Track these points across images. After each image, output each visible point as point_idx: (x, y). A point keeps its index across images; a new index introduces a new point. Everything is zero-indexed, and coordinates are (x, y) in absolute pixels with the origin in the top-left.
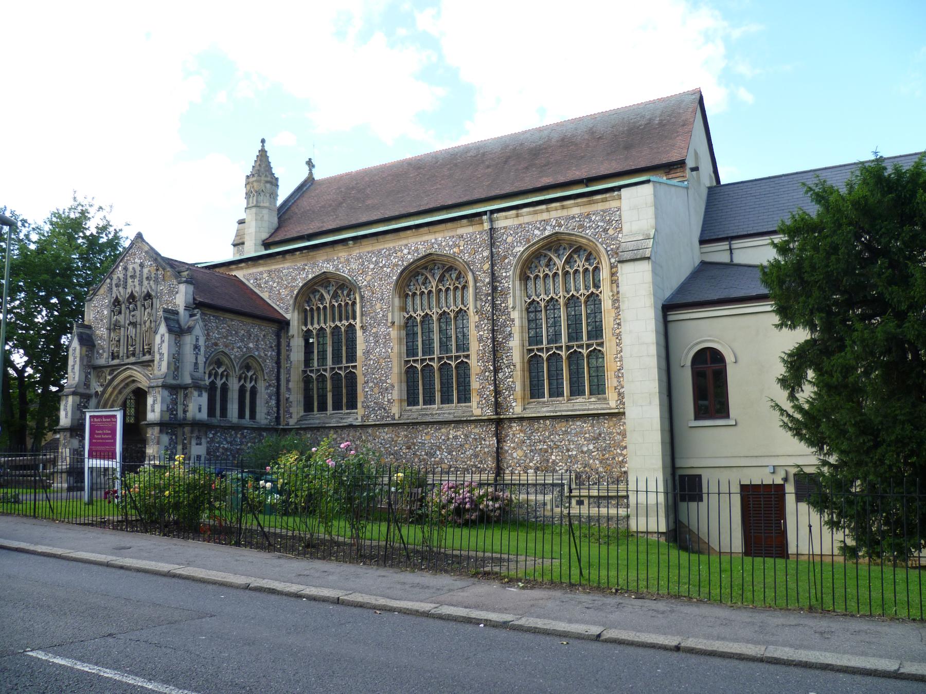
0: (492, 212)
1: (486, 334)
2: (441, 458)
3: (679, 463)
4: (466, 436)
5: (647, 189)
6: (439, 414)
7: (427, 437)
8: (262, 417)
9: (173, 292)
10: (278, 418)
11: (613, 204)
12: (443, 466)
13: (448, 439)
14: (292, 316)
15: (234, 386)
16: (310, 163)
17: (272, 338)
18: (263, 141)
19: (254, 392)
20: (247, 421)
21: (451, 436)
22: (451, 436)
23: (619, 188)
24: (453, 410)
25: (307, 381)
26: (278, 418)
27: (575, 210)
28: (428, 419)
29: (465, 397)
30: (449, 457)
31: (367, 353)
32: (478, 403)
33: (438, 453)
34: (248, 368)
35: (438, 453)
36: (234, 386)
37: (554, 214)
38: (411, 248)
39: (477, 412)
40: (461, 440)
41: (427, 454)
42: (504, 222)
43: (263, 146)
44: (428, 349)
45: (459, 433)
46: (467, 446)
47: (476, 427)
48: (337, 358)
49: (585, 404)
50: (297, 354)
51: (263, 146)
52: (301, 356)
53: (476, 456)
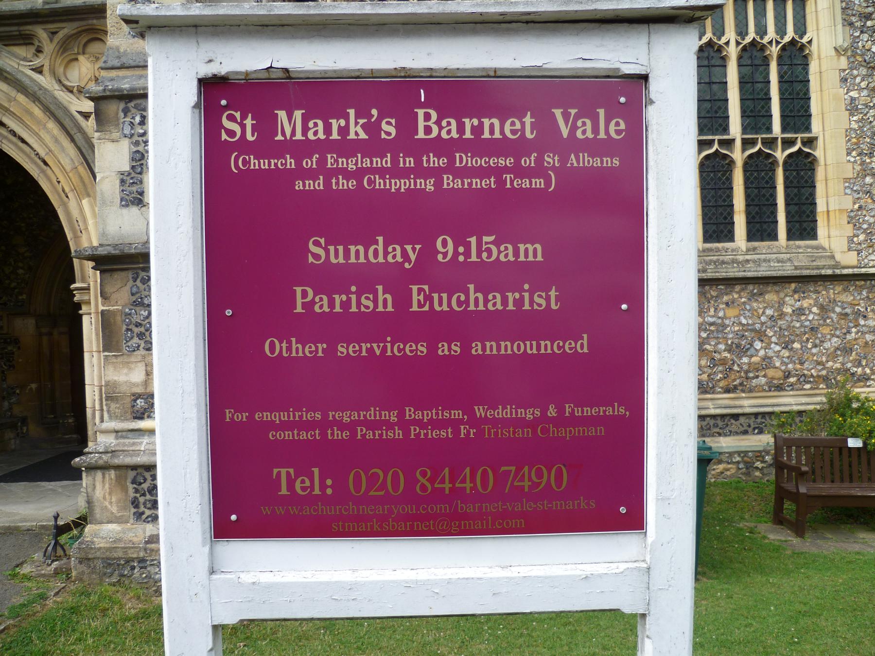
2: (765, 358)
4: (822, 308)
6: (757, 262)
7: (731, 312)
12: (771, 373)
13: (782, 315)
21: (788, 310)
22: (788, 310)
24: (782, 254)
28: (734, 272)
29: (803, 224)
30: (785, 353)
32: (850, 240)
33: (758, 345)
35: (758, 345)
39: (848, 260)
40: (813, 315)
41: (729, 350)
45: (805, 303)
46: (826, 330)
47: (845, 290)
53: (847, 350)
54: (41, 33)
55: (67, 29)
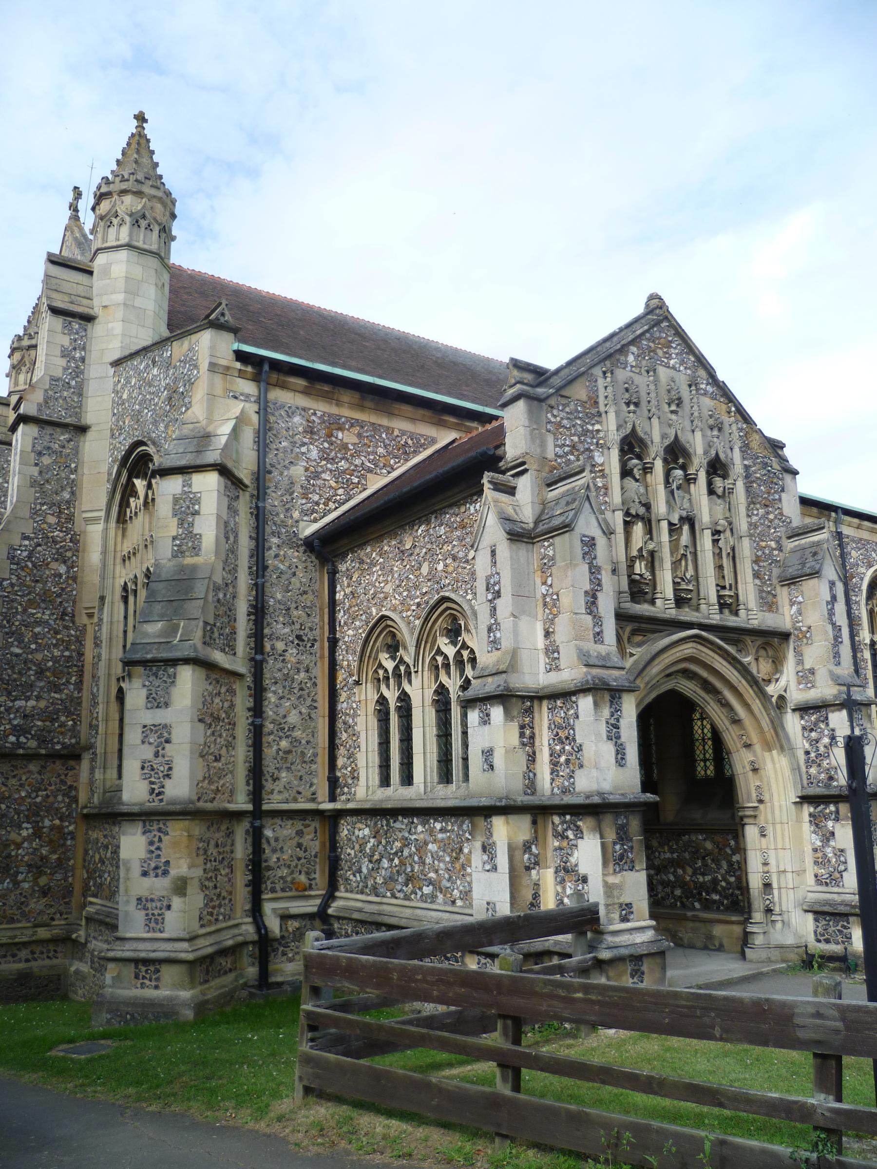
18: (141, 118)
43: (140, 127)
51: (140, 127)
54: (748, 640)
55: (759, 641)
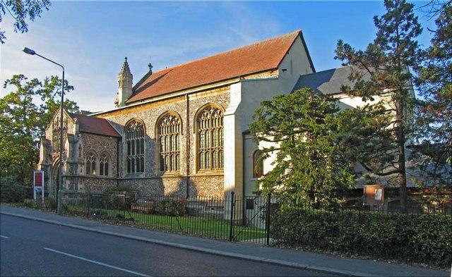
0: (188, 94)
1: (185, 143)
3: (246, 195)
5: (239, 84)
8: (111, 175)
9: (72, 127)
10: (118, 175)
11: (227, 91)
14: (123, 136)
15: (98, 163)
16: (150, 66)
17: (115, 144)
18: (126, 58)
19: (107, 165)
20: (104, 176)
23: (230, 85)
25: (129, 160)
26: (118, 175)
27: (215, 93)
31: (147, 150)
34: (104, 155)
36: (98, 163)
37: (209, 95)
38: (161, 108)
42: (192, 98)
44: (133, 153)
48: (138, 153)
49: (215, 172)
50: (125, 151)
52: (126, 151)
